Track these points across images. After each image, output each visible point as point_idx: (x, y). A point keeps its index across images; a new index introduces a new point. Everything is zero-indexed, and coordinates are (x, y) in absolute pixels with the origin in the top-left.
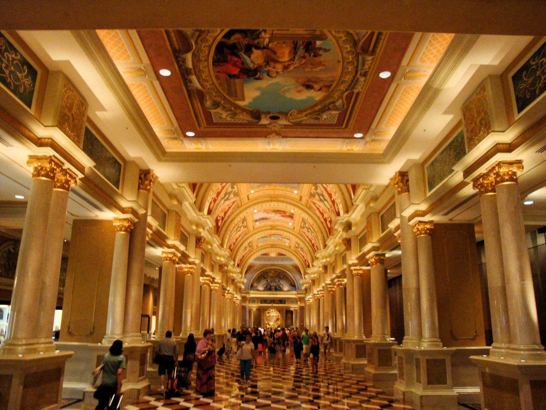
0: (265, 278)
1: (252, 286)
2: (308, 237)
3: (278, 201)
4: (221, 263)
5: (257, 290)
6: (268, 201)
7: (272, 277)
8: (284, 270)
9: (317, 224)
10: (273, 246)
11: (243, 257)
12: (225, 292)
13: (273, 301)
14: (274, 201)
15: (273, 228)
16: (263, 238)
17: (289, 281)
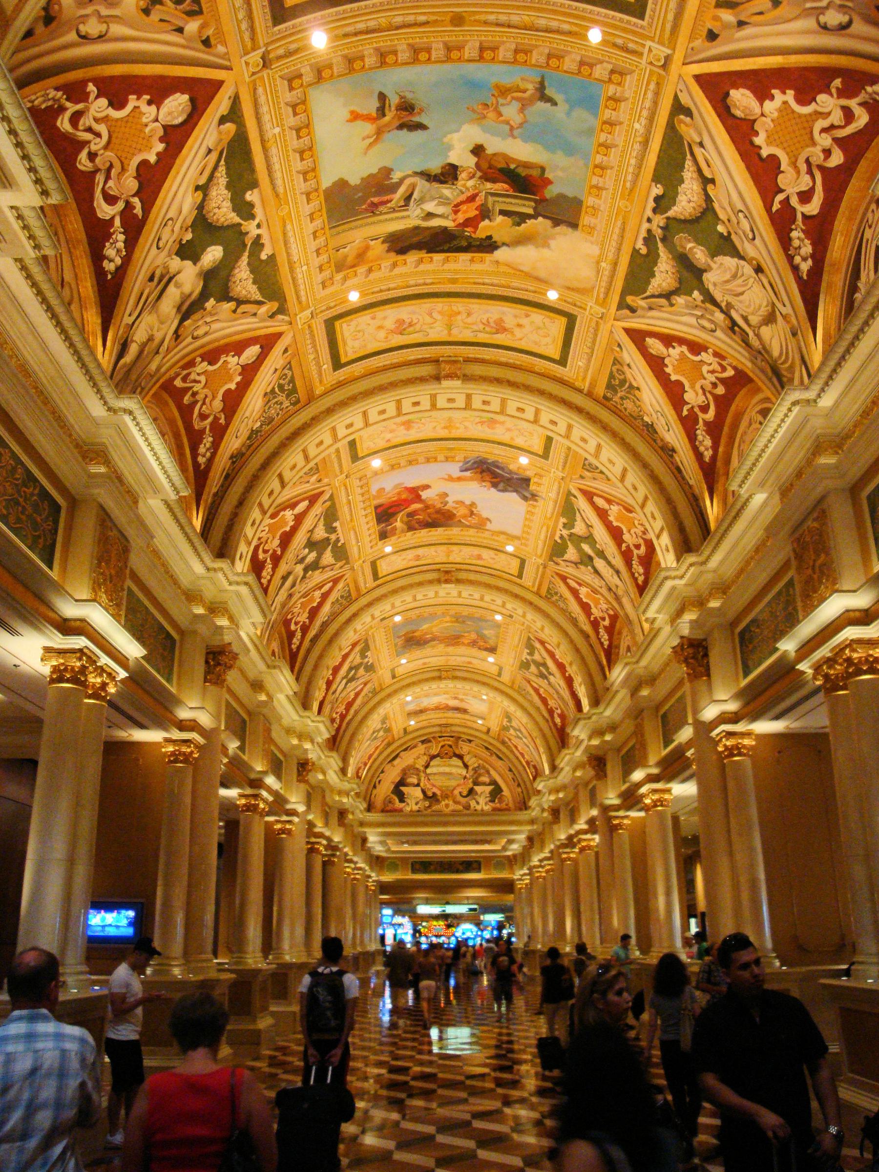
2: (575, 593)
3: (467, 378)
4: (216, 642)
6: (422, 380)
14: (450, 376)
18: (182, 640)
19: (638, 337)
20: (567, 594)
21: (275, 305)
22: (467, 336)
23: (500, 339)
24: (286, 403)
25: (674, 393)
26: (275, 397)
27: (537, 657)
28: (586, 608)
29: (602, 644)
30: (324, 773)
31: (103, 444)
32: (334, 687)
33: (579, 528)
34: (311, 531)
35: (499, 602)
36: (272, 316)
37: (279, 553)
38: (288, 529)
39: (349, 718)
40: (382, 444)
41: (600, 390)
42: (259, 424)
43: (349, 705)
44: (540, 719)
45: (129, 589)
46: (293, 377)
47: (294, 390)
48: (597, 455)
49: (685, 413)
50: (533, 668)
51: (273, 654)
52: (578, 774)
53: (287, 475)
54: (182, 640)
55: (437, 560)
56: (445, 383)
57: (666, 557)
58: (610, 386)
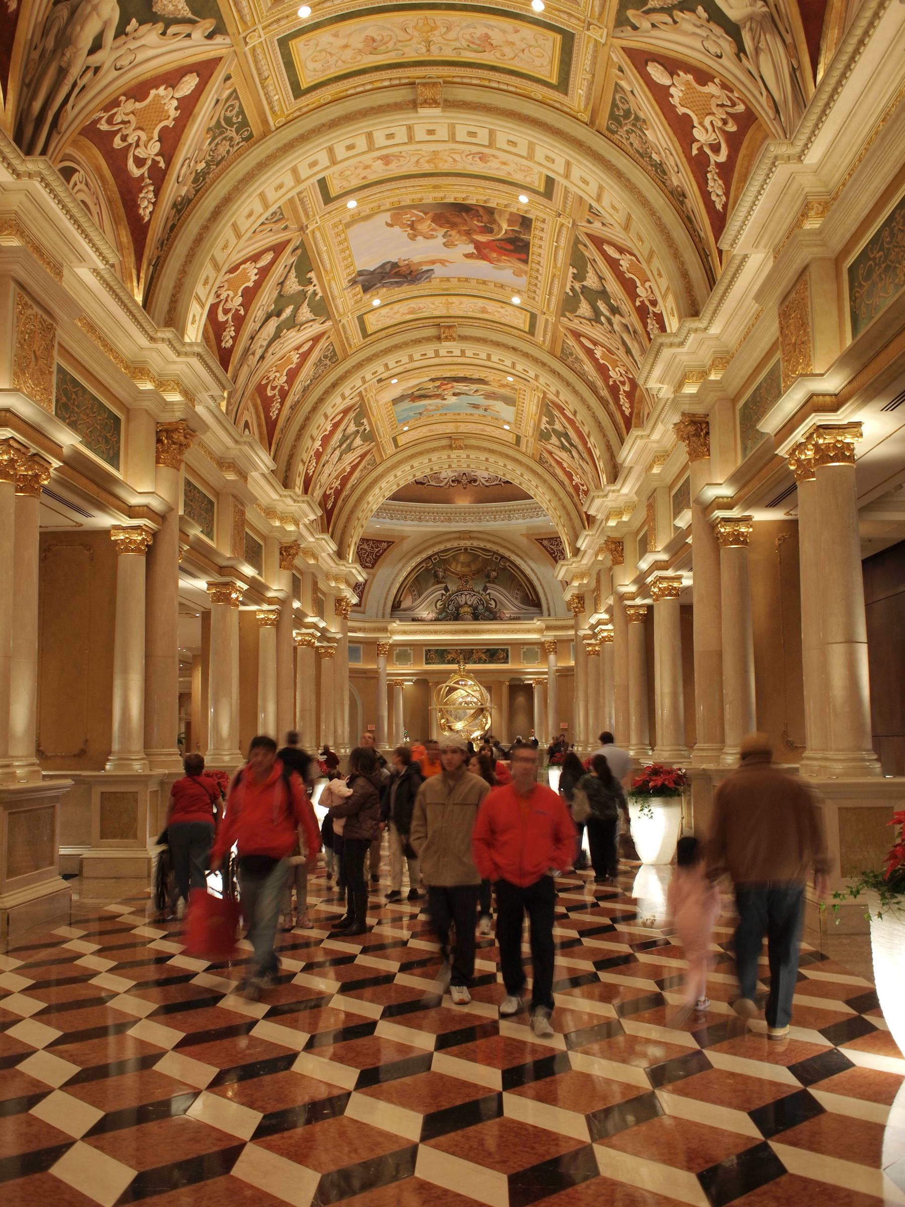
0: (439, 582)
1: (396, 606)
2: (590, 353)
3: (450, 104)
5: (414, 620)
6: (396, 107)
7: (462, 577)
8: (502, 551)
9: (652, 212)
10: (453, 442)
11: (345, 480)
12: (230, 585)
13: (467, 653)
15: (443, 329)
16: (414, 397)
17: (520, 587)
18: (128, 420)
19: (640, 59)
20: (582, 356)
21: (208, 25)
22: (448, 54)
23: (488, 58)
24: (237, 139)
25: (682, 128)
26: (222, 133)
27: (558, 426)
28: (603, 371)
29: (622, 412)
30: (316, 558)
31: (16, 213)
32: (324, 458)
33: (591, 281)
34: (282, 284)
35: (508, 363)
36: (210, 36)
37: (242, 312)
38: (250, 284)
39: (344, 494)
40: (355, 182)
41: (603, 120)
42: (203, 165)
43: (345, 480)
44: (562, 494)
45: (60, 369)
46: (241, 106)
47: (244, 124)
48: (599, 199)
49: (695, 152)
50: (554, 440)
51: (247, 425)
52: (600, 558)
53: (245, 225)
54: (128, 420)
55: (437, 313)
56: (423, 112)
57: (672, 324)
58: (613, 117)
